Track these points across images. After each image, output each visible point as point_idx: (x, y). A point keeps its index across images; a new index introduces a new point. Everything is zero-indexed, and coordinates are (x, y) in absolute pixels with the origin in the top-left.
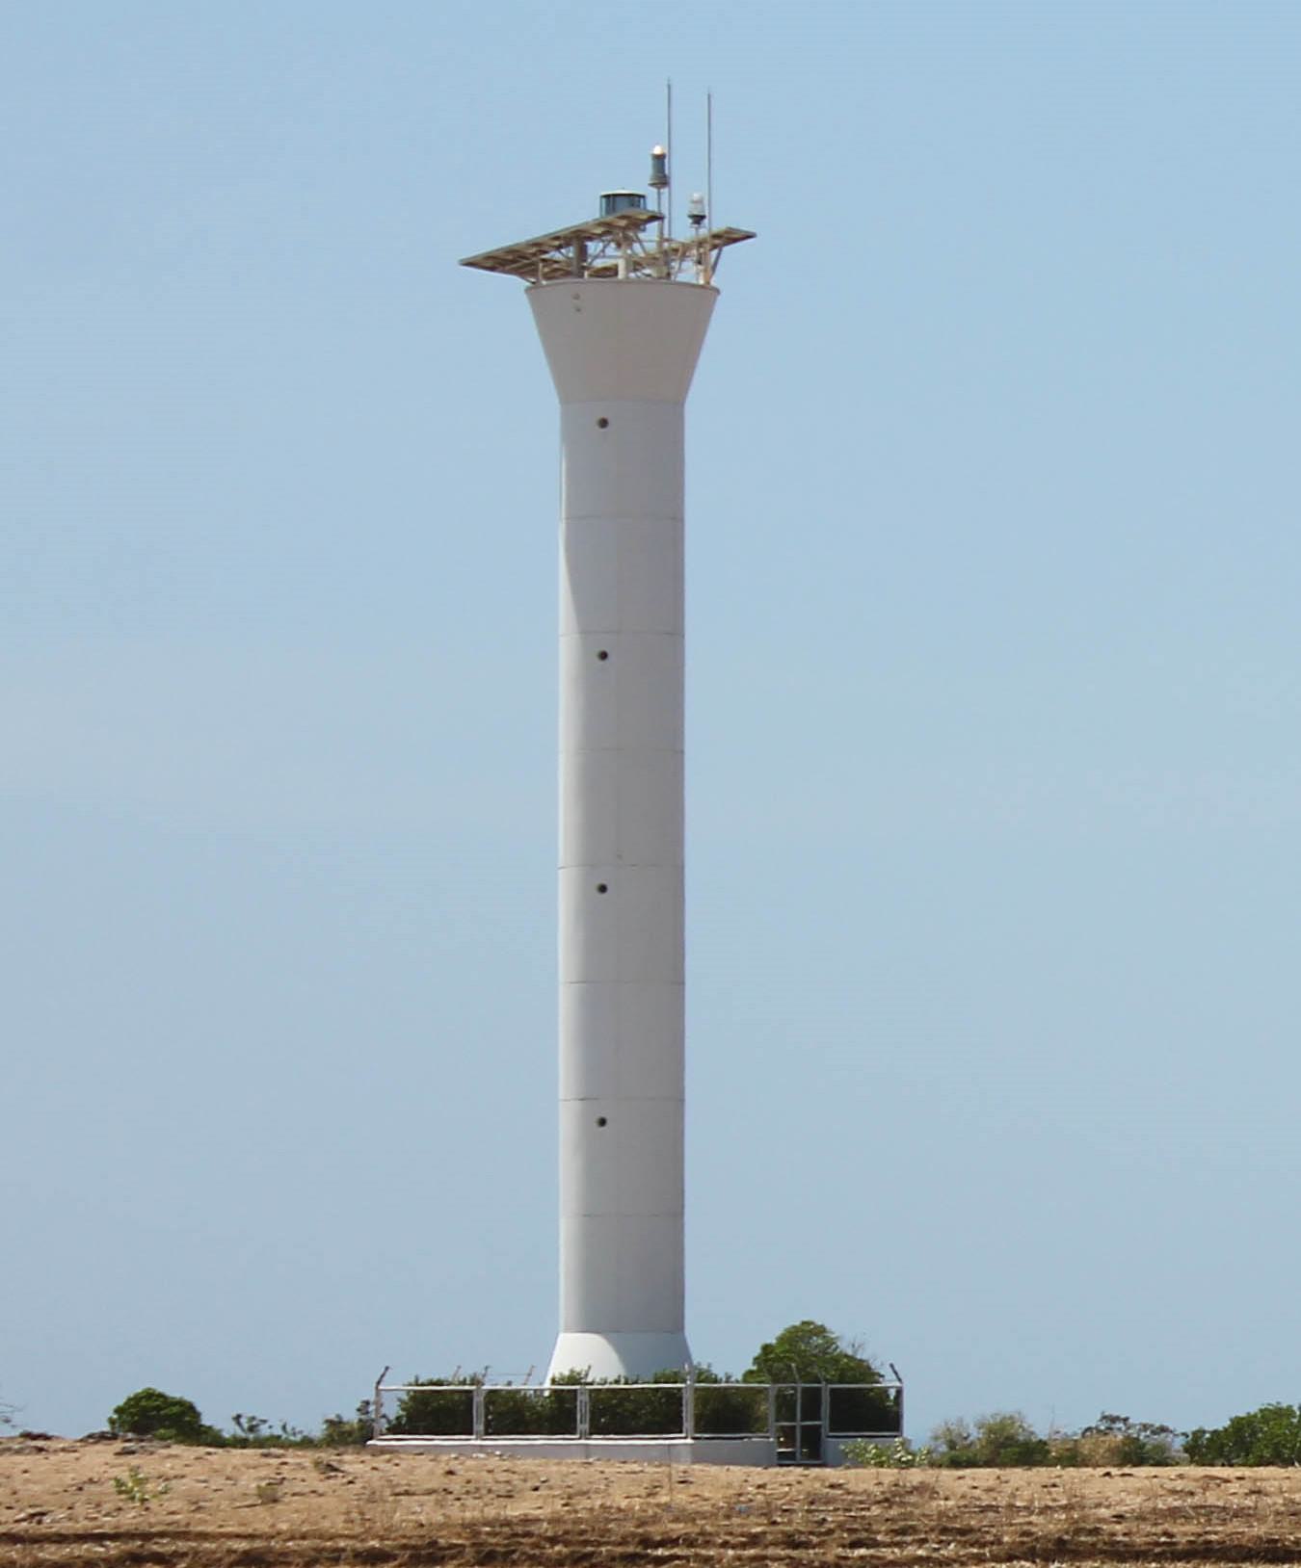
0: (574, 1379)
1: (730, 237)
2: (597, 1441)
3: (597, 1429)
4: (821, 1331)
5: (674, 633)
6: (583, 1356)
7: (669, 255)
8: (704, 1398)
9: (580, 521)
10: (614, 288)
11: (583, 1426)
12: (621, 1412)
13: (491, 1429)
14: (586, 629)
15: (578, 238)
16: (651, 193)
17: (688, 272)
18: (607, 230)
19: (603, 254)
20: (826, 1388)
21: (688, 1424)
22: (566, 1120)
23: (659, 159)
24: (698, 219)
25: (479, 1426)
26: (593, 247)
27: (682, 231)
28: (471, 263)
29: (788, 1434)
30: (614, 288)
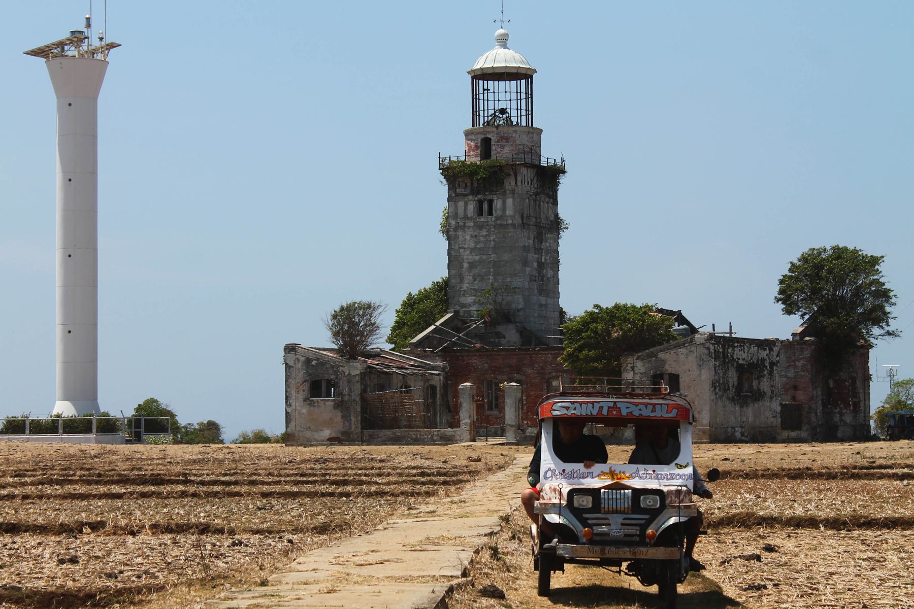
0: (59, 416)
1: (112, 46)
2: (65, 436)
3: (65, 432)
4: (156, 401)
5: (94, 173)
6: (65, 409)
7: (93, 53)
8: (99, 422)
9: (61, 136)
10: (75, 61)
11: (27, 431)
12: (72, 427)
13: (31, 432)
14: (64, 172)
15: (61, 45)
16: (85, 30)
17: (99, 56)
18: (71, 42)
19: (71, 51)
20: (143, 419)
21: (94, 430)
22: (58, 331)
23: (88, 19)
24: (101, 39)
25: (27, 431)
26: (66, 48)
27: (96, 43)
28: (26, 53)
29: (130, 434)
30: (75, 61)
